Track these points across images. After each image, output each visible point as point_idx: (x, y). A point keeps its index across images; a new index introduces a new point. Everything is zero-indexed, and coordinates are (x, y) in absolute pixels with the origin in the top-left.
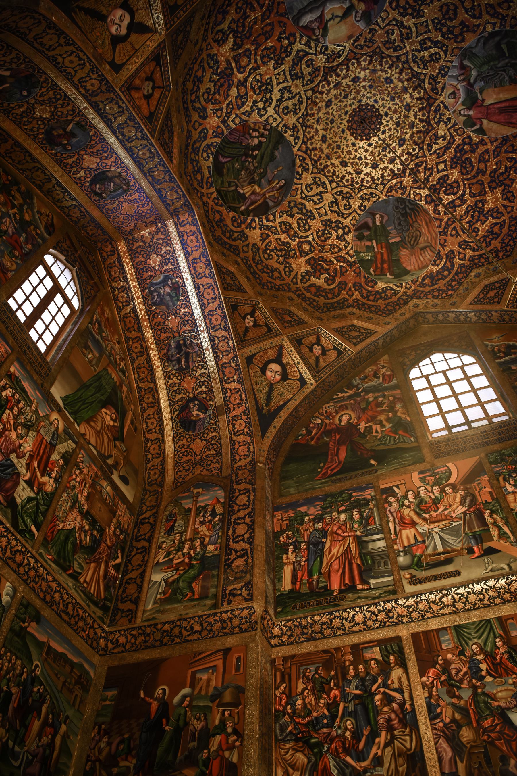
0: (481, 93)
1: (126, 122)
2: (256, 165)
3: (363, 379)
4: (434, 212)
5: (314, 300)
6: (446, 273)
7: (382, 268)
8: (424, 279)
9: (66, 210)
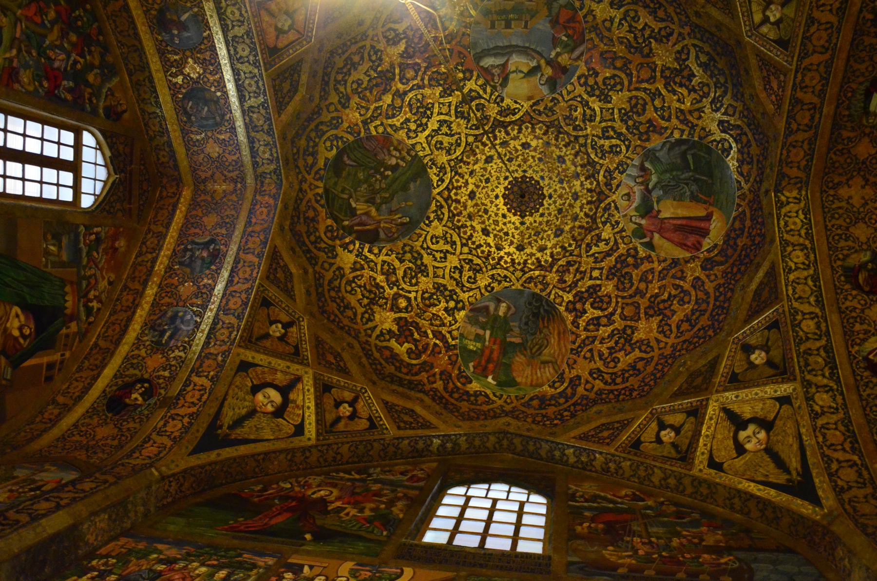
0: (658, 202)
1: (242, 37)
2: (384, 186)
3: (384, 472)
4: (573, 322)
5: (381, 364)
6: (562, 400)
7: (485, 369)
8: (532, 399)
9: (146, 117)
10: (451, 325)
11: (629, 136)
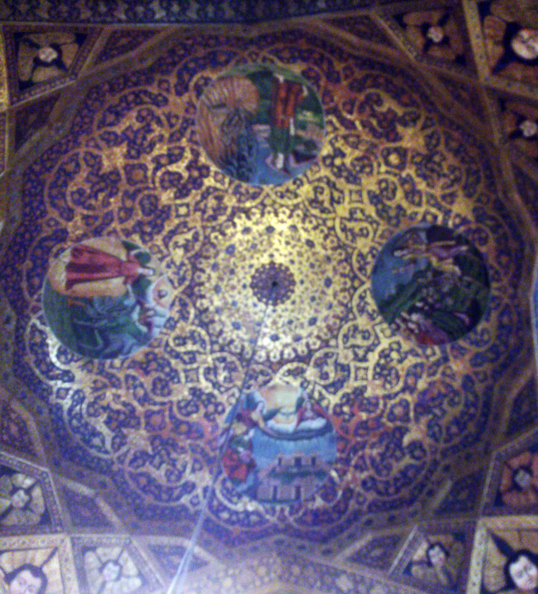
10: (336, 138)
11: (167, 356)
